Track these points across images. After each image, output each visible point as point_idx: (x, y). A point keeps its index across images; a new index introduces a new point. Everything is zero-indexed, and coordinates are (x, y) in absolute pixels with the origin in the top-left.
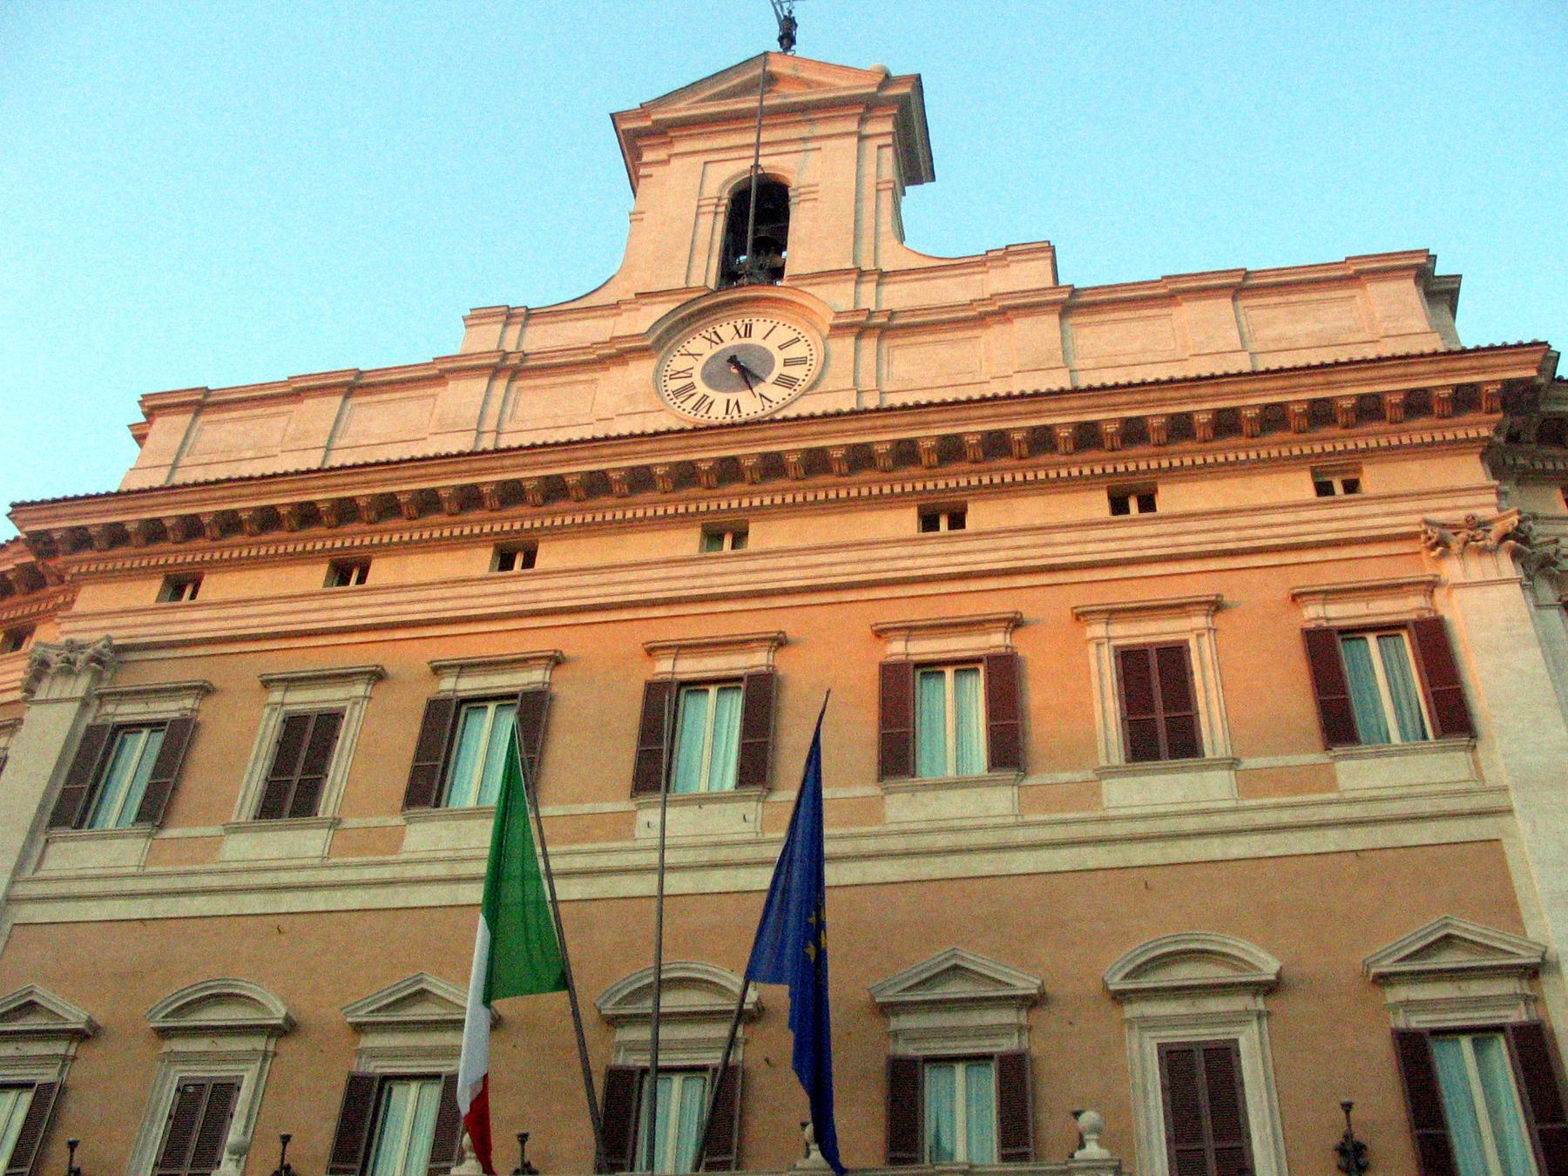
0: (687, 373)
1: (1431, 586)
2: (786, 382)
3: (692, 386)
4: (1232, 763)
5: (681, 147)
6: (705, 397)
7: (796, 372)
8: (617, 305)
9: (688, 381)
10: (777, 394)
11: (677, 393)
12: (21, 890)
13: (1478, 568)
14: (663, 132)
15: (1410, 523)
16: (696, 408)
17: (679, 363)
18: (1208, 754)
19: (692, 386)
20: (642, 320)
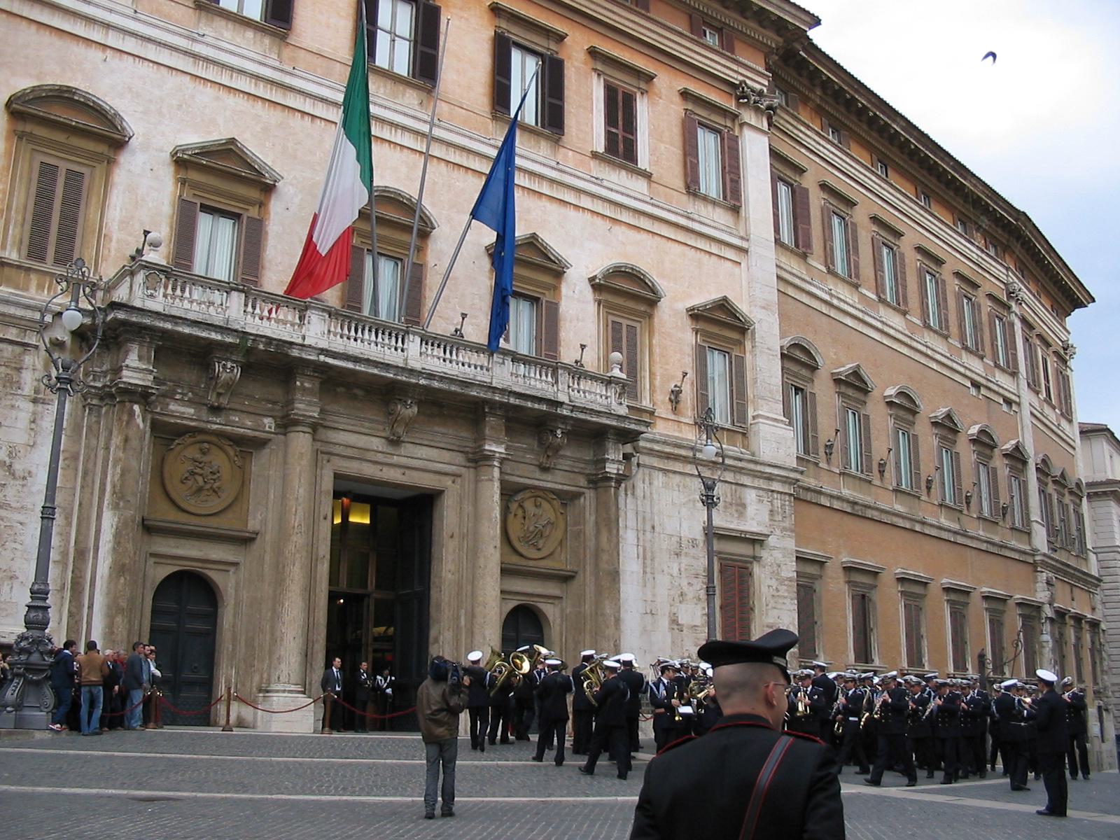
1: (735, 117)
4: (647, 176)
15: (736, 78)
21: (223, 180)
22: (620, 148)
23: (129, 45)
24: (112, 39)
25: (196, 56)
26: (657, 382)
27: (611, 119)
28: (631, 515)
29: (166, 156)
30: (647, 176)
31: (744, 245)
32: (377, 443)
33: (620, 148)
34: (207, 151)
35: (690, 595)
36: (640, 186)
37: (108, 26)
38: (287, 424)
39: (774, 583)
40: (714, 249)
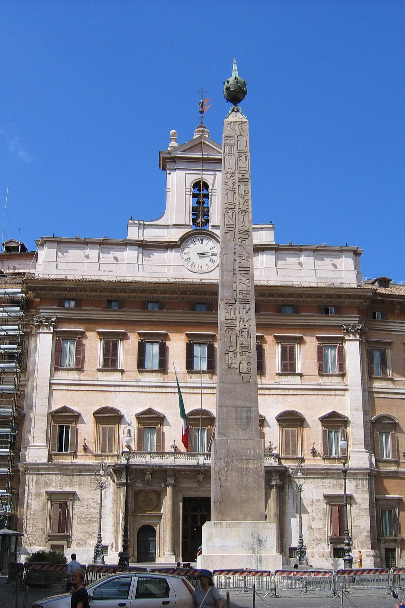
0: (187, 254)
2: (213, 261)
3: (189, 258)
4: (301, 375)
5: (179, 165)
6: (193, 263)
7: (214, 258)
8: (168, 226)
9: (188, 256)
10: (210, 264)
11: (187, 260)
12: (52, 381)
13: (352, 337)
14: (174, 159)
16: (191, 266)
17: (187, 250)
18: (297, 372)
19: (189, 258)
20: (175, 235)
21: (150, 420)
22: (289, 368)
23: (121, 389)
24: (117, 389)
25: (139, 386)
26: (305, 447)
27: (284, 358)
28: (290, 494)
29: (134, 417)
30: (301, 375)
31: (346, 387)
32: (195, 485)
33: (289, 368)
34: (143, 413)
35: (317, 517)
36: (297, 379)
37: (115, 386)
38: (167, 486)
39: (358, 511)
40: (332, 393)
